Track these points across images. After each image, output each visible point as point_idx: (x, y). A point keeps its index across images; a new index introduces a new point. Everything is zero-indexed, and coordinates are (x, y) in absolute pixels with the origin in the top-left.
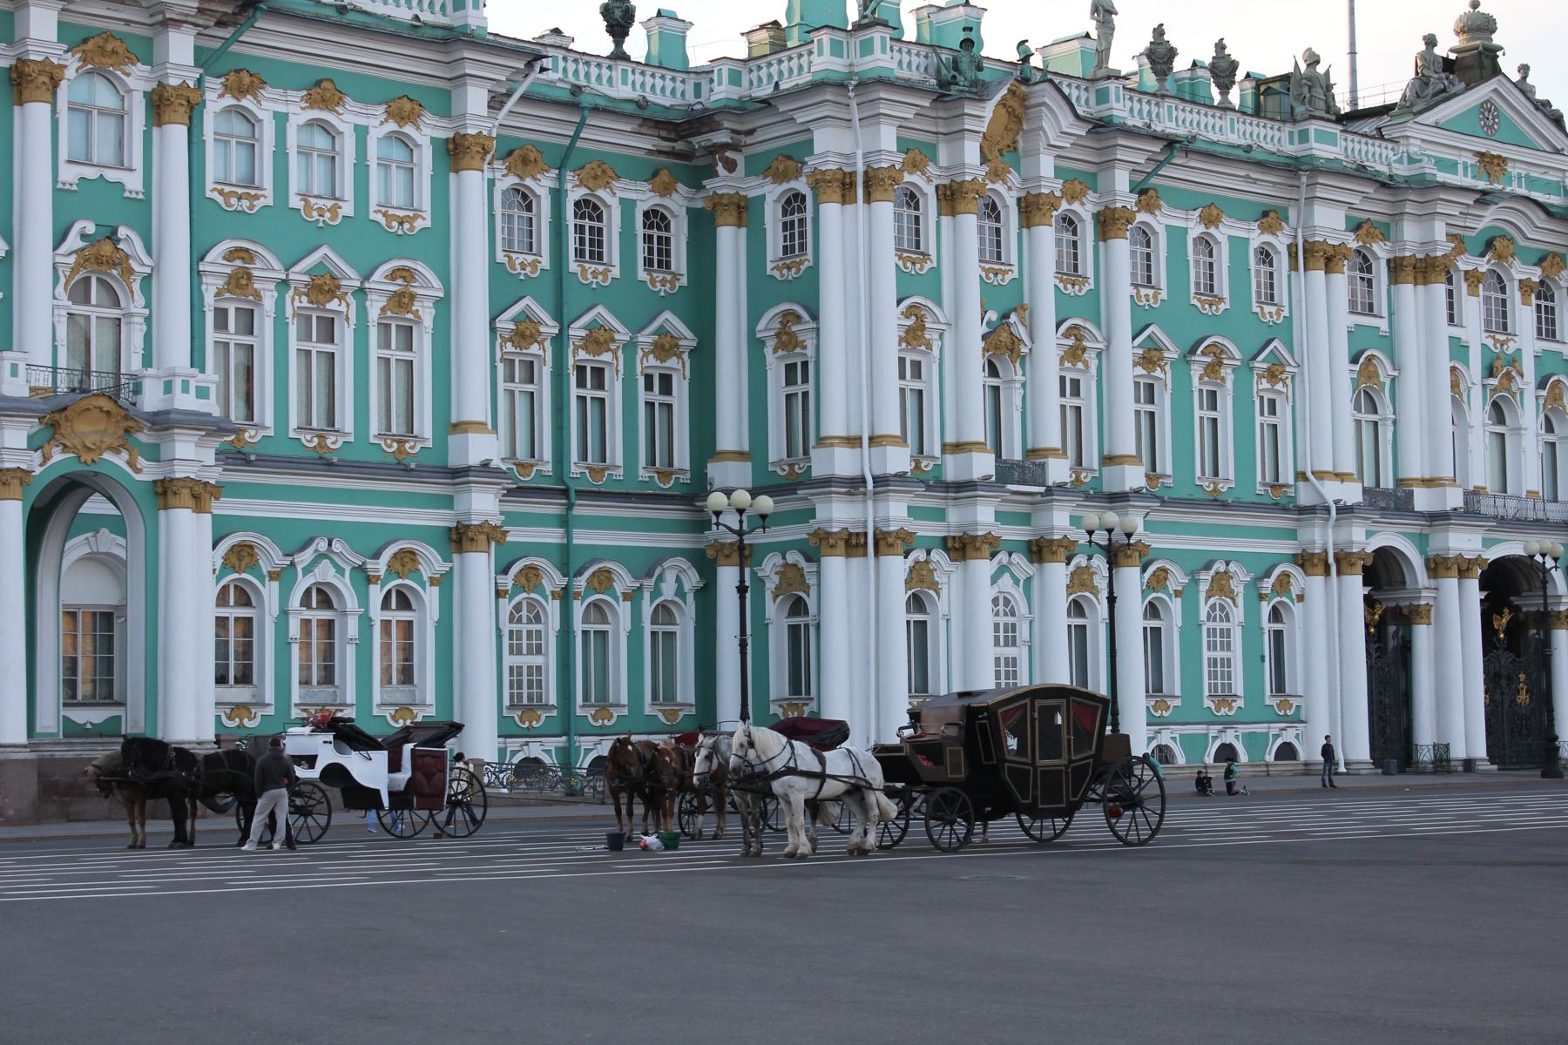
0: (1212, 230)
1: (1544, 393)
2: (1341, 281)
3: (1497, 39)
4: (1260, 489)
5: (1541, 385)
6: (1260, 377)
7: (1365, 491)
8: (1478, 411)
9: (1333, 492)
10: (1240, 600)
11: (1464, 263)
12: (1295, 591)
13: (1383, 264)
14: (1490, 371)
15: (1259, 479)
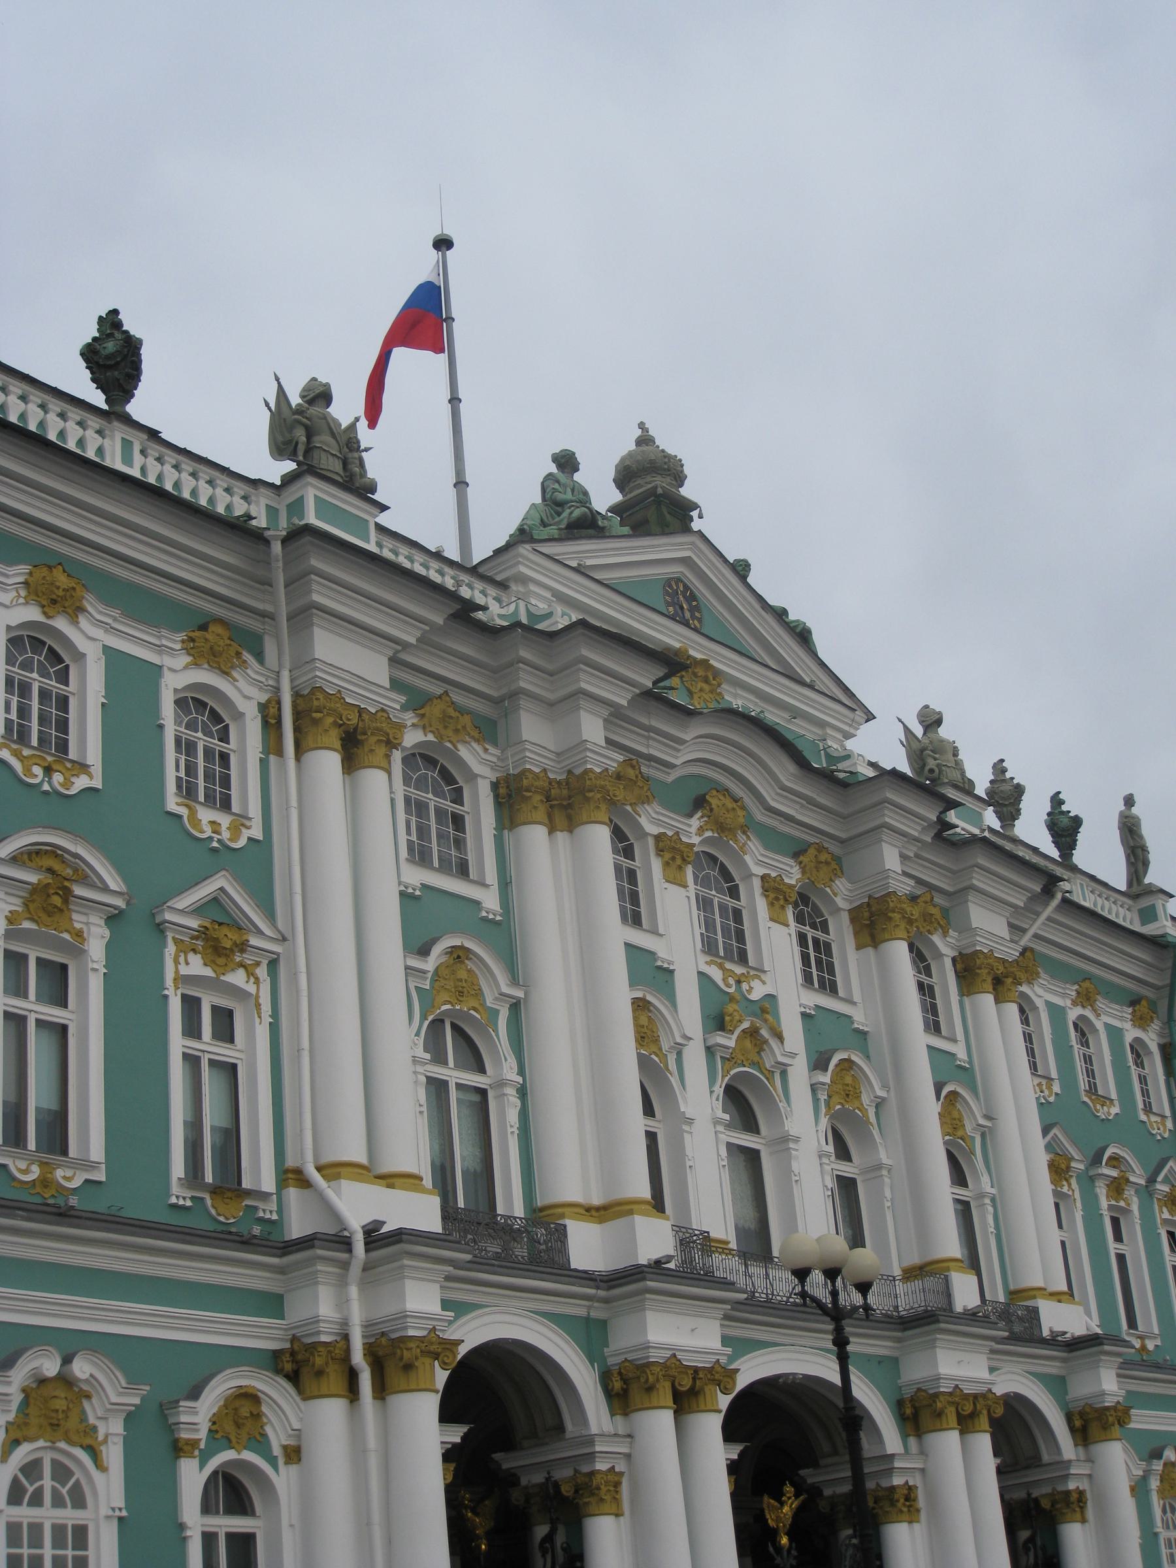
0: (61, 623)
1: (826, 1078)
2: (382, 787)
3: (686, 491)
4: (179, 1194)
5: (819, 1063)
6: (184, 948)
7: (449, 1213)
8: (699, 1098)
9: (358, 1204)
10: (114, 1454)
11: (652, 820)
12: (277, 1439)
13: (484, 791)
14: (718, 1022)
15: (178, 1168)
